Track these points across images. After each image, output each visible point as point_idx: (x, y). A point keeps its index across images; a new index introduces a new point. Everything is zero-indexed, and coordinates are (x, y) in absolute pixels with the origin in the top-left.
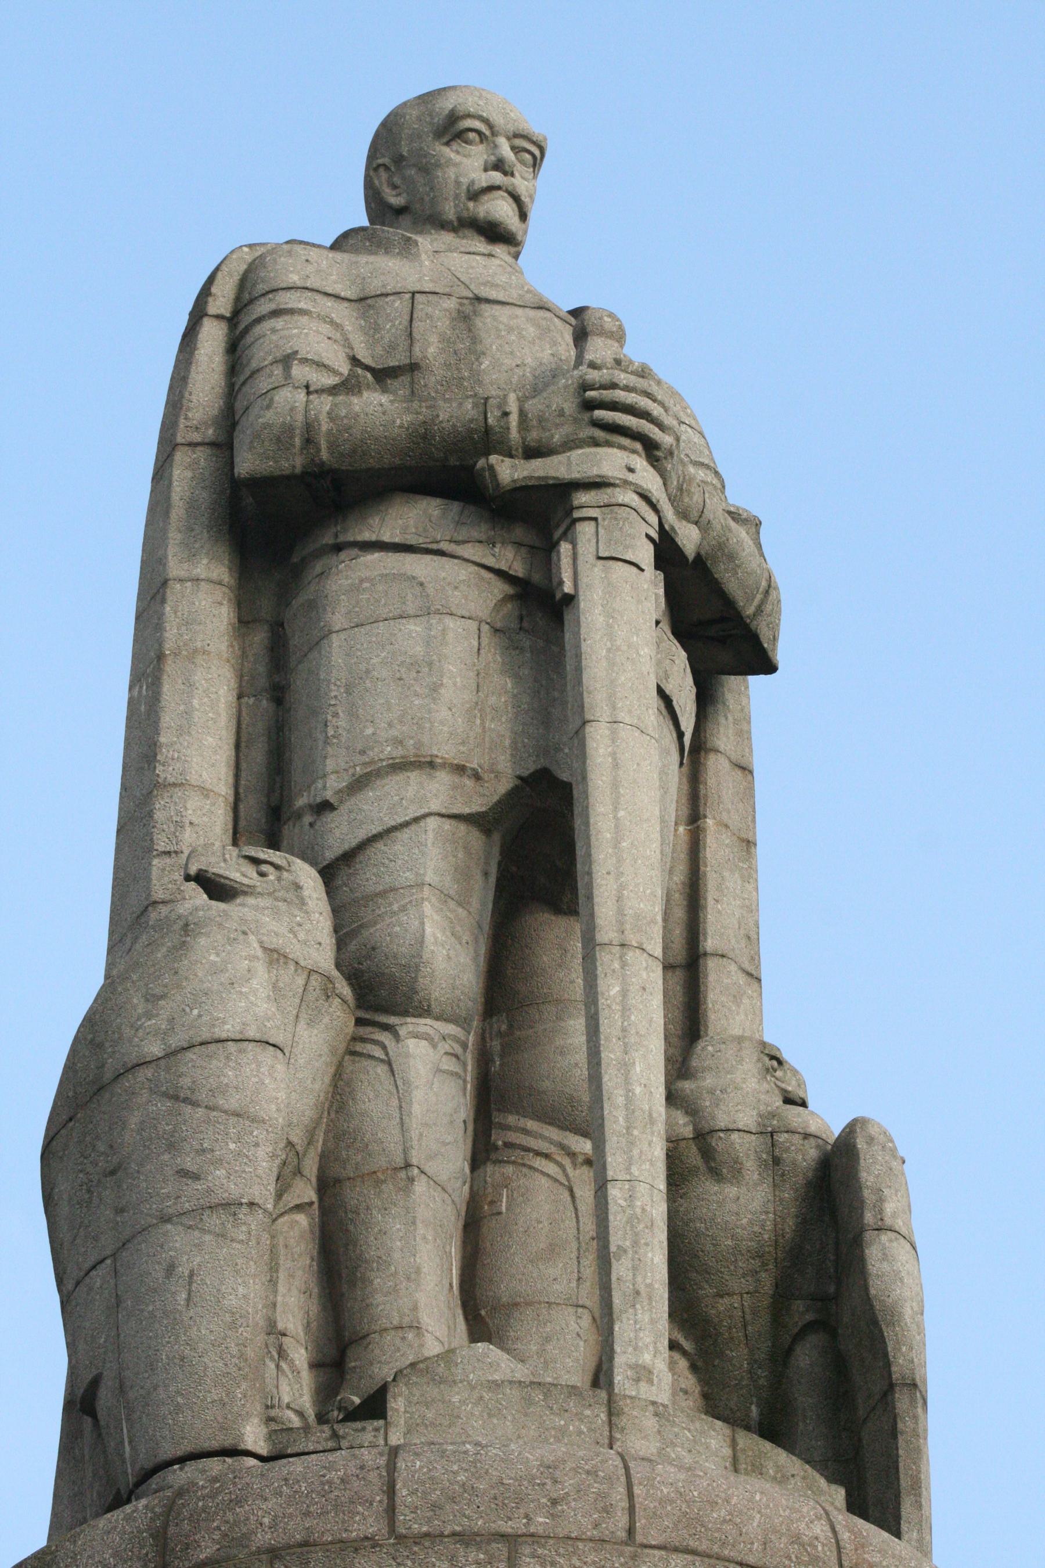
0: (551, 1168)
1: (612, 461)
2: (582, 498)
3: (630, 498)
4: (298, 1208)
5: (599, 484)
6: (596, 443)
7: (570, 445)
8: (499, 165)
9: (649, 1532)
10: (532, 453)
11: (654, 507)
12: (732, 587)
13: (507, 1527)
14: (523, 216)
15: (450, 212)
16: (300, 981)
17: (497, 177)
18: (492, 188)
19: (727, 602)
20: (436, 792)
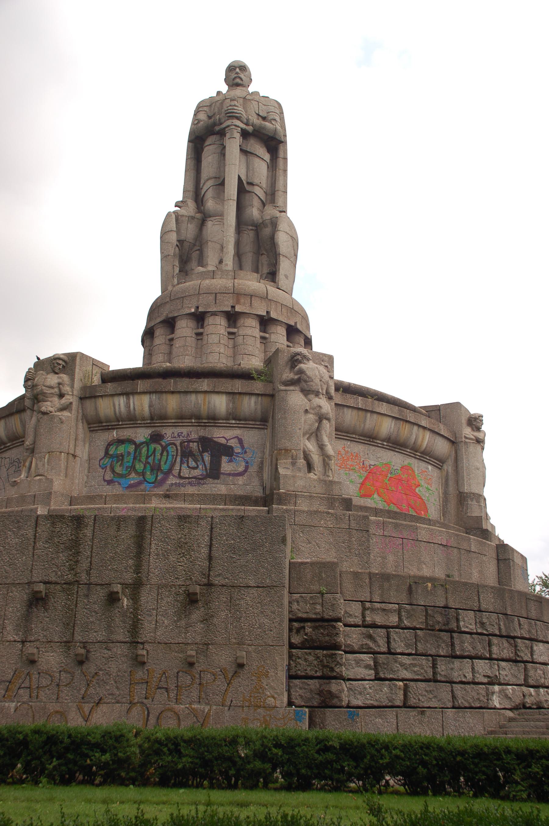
0: (246, 232)
1: (229, 123)
2: (227, 129)
3: (234, 127)
4: (196, 250)
5: (228, 126)
6: (228, 120)
7: (225, 122)
8: (237, 73)
9: (201, 292)
10: (221, 124)
11: (238, 127)
12: (267, 133)
13: (182, 296)
14: (242, 80)
15: (231, 83)
16: (187, 218)
17: (236, 75)
18: (235, 78)
19: (267, 135)
20: (210, 183)
